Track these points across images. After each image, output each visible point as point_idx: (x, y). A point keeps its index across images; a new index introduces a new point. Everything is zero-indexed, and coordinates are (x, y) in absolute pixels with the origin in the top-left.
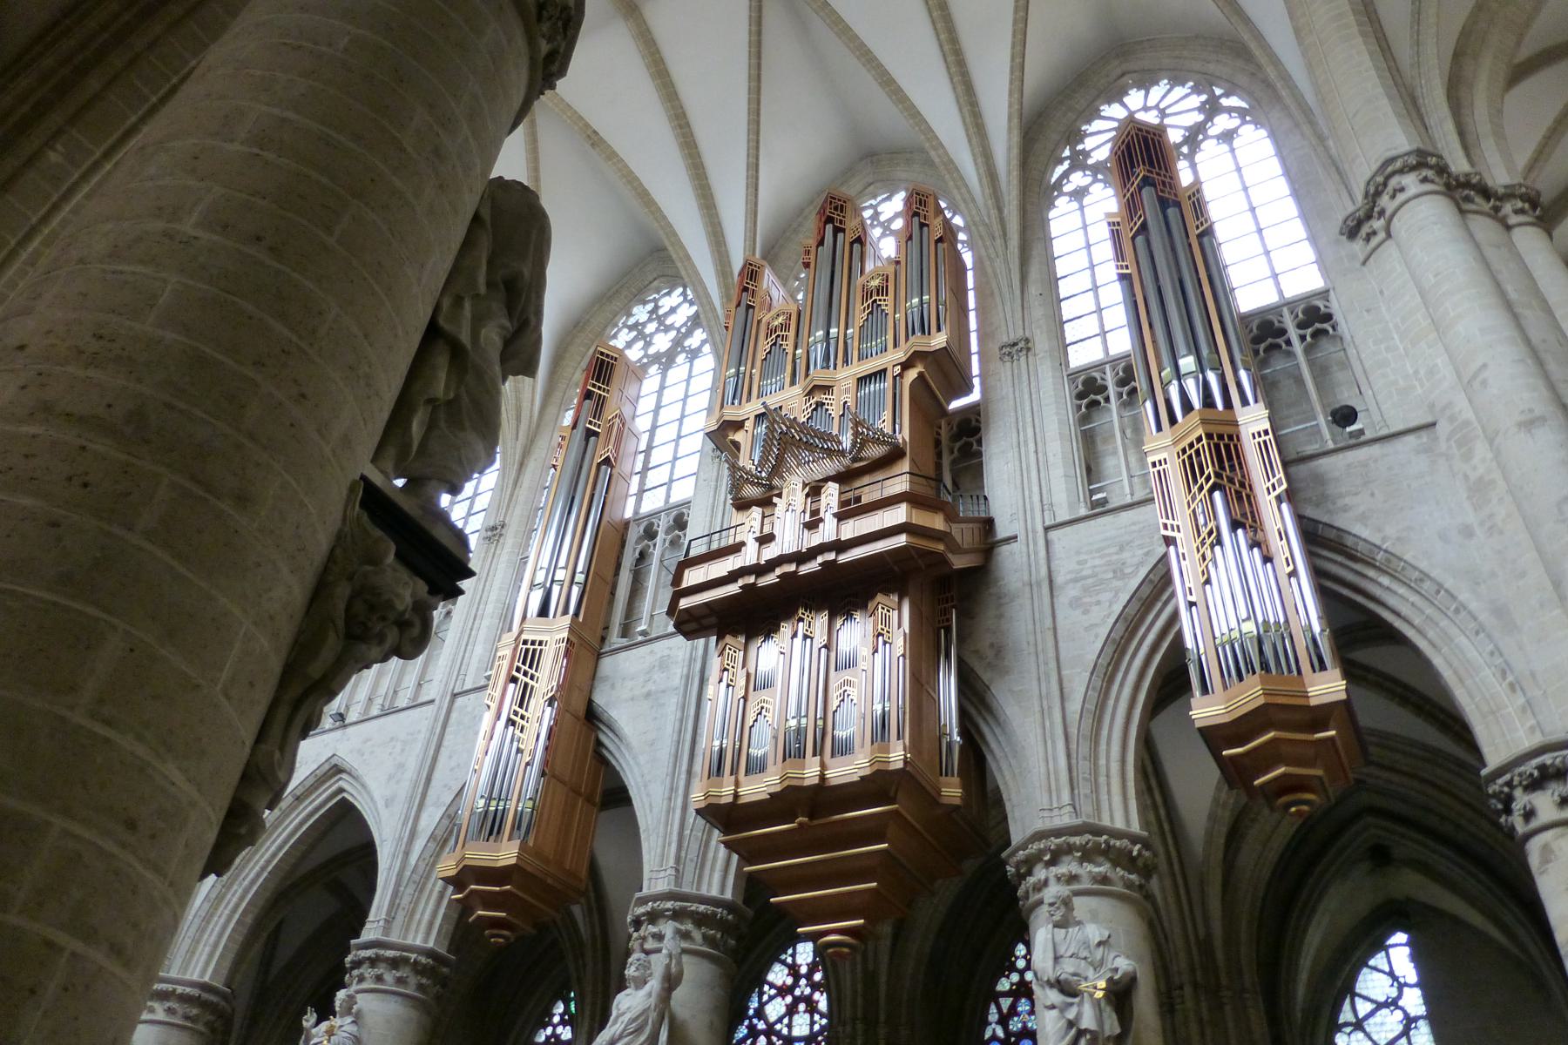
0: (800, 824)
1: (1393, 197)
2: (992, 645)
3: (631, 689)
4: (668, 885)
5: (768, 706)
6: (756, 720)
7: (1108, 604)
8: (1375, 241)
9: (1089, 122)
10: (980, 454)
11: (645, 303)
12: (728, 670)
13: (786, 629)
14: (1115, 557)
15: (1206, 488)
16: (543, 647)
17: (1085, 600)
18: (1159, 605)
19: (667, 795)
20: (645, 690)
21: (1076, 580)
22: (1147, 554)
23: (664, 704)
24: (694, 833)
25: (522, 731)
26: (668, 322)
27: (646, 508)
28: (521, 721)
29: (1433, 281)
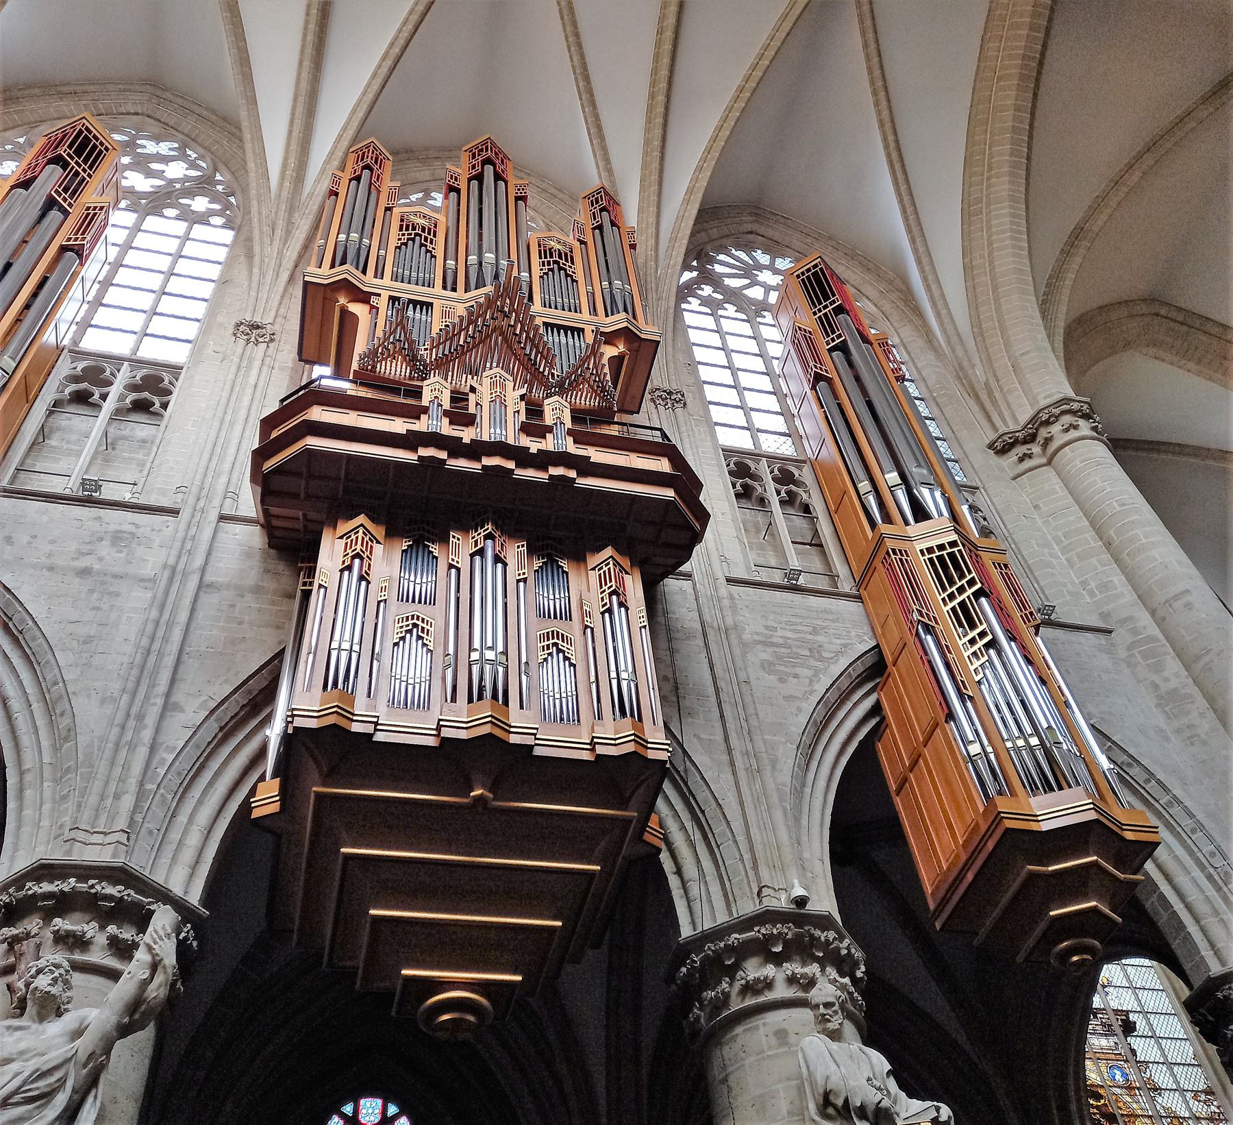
0: (479, 798)
1: (1067, 430)
3: (50, 555)
4: (114, 856)
6: (403, 638)
7: (807, 681)
8: (1028, 464)
9: (719, 252)
12: (362, 559)
15: (970, 592)
17: (782, 668)
18: (849, 705)
19: (119, 718)
20: (84, 563)
22: (845, 646)
23: (117, 595)
24: (162, 791)
26: (155, 166)
27: (93, 342)
29: (1118, 509)
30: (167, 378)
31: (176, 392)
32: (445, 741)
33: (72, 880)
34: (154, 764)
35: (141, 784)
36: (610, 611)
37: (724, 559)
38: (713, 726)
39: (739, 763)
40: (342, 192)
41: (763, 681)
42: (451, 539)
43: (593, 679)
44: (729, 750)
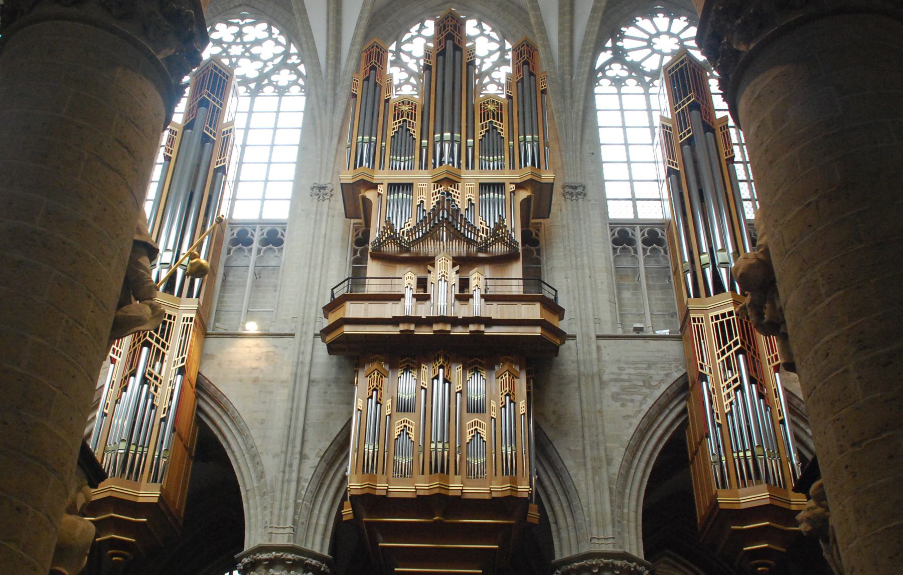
2: (554, 412)
4: (289, 540)
5: (411, 427)
6: (399, 435)
7: (638, 403)
10: (539, 262)
11: (229, 24)
13: (427, 371)
14: (645, 371)
16: (172, 321)
17: (623, 397)
21: (616, 380)
22: (667, 375)
23: (271, 392)
24: (305, 502)
25: (156, 390)
26: (255, 50)
28: (155, 382)
30: (280, 230)
31: (285, 240)
32: (418, 496)
33: (274, 553)
34: (300, 489)
35: (295, 501)
36: (505, 406)
37: (598, 321)
38: (578, 441)
39: (589, 466)
40: (359, 93)
41: (611, 407)
42: (422, 369)
43: (493, 451)
44: (585, 458)
